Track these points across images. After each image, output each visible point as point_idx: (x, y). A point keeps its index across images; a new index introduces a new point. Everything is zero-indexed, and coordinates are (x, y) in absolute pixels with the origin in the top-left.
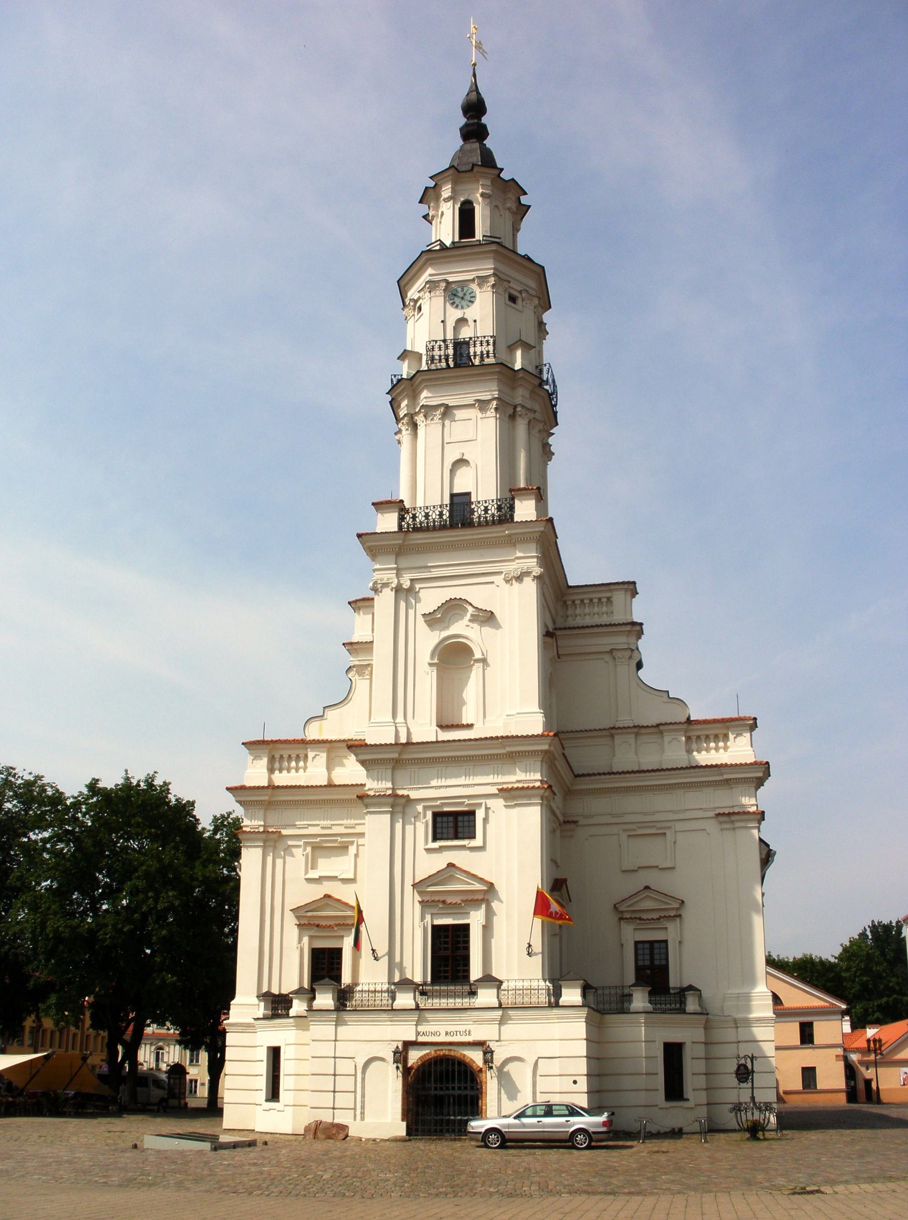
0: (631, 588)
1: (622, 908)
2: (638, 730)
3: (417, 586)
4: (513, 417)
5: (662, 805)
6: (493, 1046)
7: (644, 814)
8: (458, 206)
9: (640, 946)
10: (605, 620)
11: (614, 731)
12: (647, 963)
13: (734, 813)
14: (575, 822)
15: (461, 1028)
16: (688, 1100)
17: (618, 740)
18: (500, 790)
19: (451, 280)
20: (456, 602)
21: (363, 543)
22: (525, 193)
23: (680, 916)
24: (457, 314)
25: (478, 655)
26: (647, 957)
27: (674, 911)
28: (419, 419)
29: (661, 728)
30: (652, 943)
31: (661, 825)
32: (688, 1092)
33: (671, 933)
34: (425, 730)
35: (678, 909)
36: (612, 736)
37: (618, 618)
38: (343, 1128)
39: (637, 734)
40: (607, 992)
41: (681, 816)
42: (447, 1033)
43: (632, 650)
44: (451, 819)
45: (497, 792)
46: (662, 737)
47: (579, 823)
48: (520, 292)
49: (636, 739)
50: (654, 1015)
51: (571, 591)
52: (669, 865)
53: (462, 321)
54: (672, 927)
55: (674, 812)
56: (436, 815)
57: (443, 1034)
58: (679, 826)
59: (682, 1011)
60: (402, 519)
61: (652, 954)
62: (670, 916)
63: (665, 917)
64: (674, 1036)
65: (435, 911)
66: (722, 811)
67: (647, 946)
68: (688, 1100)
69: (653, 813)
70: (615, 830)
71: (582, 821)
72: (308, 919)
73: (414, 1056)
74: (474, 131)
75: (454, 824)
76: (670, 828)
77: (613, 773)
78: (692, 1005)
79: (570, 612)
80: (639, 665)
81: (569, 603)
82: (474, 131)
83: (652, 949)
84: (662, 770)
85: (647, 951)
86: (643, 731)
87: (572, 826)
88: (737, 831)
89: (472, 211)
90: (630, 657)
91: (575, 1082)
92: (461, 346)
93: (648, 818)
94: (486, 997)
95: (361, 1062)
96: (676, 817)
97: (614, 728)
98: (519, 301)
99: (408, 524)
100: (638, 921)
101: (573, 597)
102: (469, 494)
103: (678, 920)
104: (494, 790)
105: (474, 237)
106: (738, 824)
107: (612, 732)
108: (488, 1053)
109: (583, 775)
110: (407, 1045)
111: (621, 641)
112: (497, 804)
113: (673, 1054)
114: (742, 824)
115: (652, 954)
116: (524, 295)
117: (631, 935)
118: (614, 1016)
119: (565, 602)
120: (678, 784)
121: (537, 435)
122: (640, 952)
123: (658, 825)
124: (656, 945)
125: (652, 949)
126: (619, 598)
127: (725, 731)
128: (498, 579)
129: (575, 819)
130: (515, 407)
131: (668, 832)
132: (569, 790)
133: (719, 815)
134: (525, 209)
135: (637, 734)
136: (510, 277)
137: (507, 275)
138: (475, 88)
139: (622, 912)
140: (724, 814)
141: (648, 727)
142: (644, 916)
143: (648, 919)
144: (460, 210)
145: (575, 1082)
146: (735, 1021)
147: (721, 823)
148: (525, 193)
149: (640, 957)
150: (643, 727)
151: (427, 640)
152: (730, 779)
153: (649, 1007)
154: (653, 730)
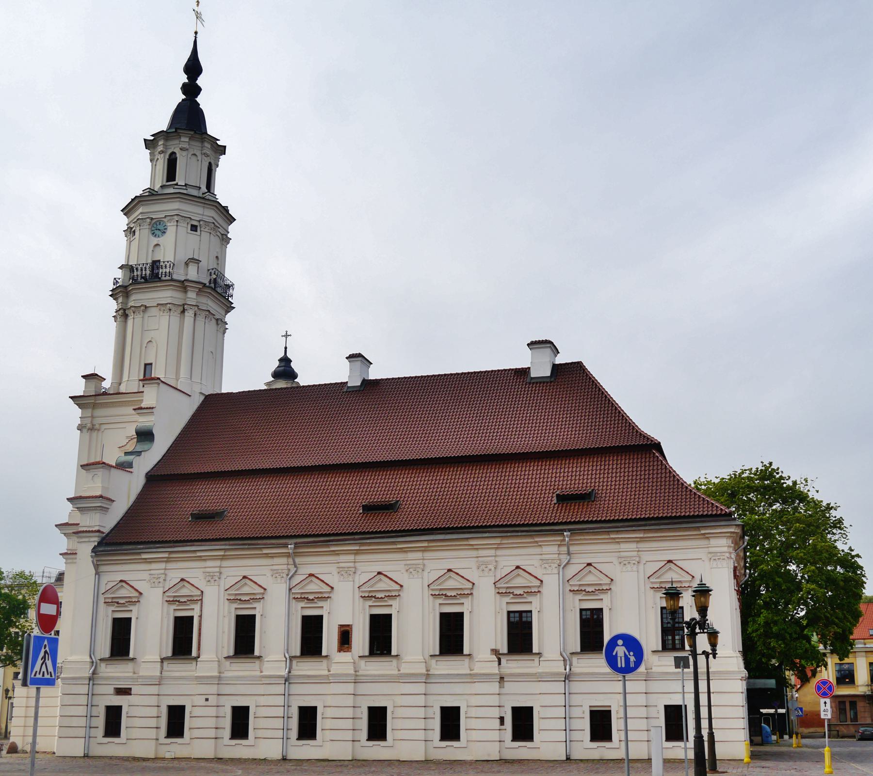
4: (183, 311)
8: (167, 157)
24: (155, 241)
28: (130, 313)
48: (199, 221)
53: (157, 245)
74: (191, 90)
82: (191, 90)
89: (176, 159)
92: (155, 264)
105: (174, 180)
144: (169, 160)
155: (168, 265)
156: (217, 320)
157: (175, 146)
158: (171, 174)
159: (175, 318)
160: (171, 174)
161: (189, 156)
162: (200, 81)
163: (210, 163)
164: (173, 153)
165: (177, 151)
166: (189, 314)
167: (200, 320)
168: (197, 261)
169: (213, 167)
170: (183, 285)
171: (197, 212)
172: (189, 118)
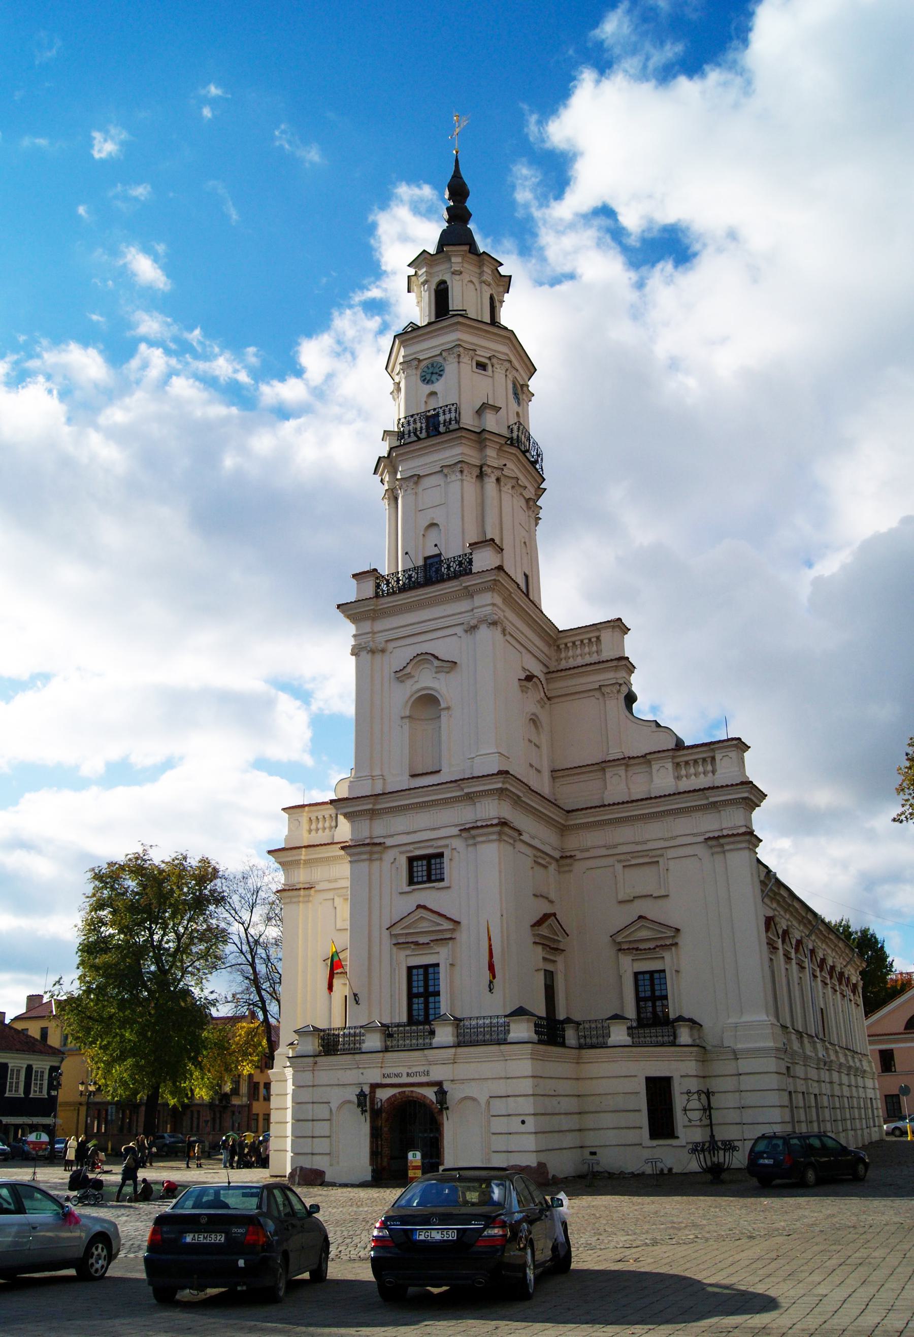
0: (618, 626)
1: (619, 939)
2: (627, 761)
3: (391, 646)
4: (481, 476)
5: (653, 833)
6: (446, 1086)
7: (637, 843)
8: (434, 287)
9: (640, 977)
10: (595, 658)
11: (604, 765)
12: (648, 994)
13: (724, 836)
14: (571, 856)
15: (421, 1069)
16: (678, 1137)
17: (609, 773)
18: (460, 830)
19: (421, 358)
21: (343, 612)
22: (501, 264)
23: (676, 944)
24: (428, 389)
25: (443, 705)
26: (648, 988)
27: (669, 938)
29: (648, 757)
30: (652, 973)
31: (654, 853)
32: (680, 1130)
33: (668, 962)
34: (399, 780)
35: (674, 937)
36: (603, 770)
37: (607, 654)
38: (321, 1174)
39: (627, 766)
40: (587, 1026)
41: (672, 843)
42: (408, 1075)
43: (620, 685)
44: (425, 862)
45: (458, 833)
46: (651, 767)
47: (577, 858)
48: (490, 358)
49: (626, 771)
50: (634, 1049)
51: (561, 635)
52: (663, 893)
53: (433, 394)
54: (667, 955)
55: (665, 839)
56: (411, 860)
57: (405, 1075)
58: (671, 853)
59: (673, 1044)
60: (378, 586)
61: (652, 984)
62: (666, 945)
63: (662, 946)
64: (658, 1069)
65: (408, 952)
66: (711, 835)
67: (647, 976)
68: (678, 1137)
69: (645, 842)
70: (610, 861)
71: (579, 855)
75: (426, 868)
76: (662, 855)
77: (605, 806)
78: (684, 1036)
79: (563, 655)
80: (631, 698)
81: (562, 646)
83: (652, 980)
84: (651, 798)
85: (647, 982)
86: (632, 762)
87: (568, 861)
88: (728, 855)
89: (446, 290)
90: (619, 691)
91: (523, 1122)
93: (639, 848)
94: (444, 1034)
95: (334, 1105)
96: (667, 844)
97: (605, 762)
98: (490, 367)
99: (383, 591)
100: (634, 952)
101: (565, 641)
102: (440, 555)
103: (673, 948)
104: (455, 831)
106: (727, 847)
107: (603, 766)
108: (442, 1093)
109: (573, 811)
110: (374, 1087)
111: (609, 677)
113: (659, 1090)
114: (731, 847)
115: (652, 984)
116: (494, 361)
117: (629, 966)
118: (588, 1051)
119: (558, 646)
120: (667, 811)
121: (510, 491)
122: (641, 983)
123: (651, 854)
124: (656, 975)
125: (652, 980)
126: (606, 636)
127: (710, 754)
128: (459, 630)
129: (573, 853)
130: (481, 467)
131: (661, 860)
132: (564, 826)
133: (709, 838)
134: (507, 279)
135: (627, 766)
136: (476, 345)
137: (472, 344)
138: (457, 175)
139: (619, 943)
140: (714, 838)
141: (638, 757)
142: (642, 946)
143: (645, 949)
145: (523, 1122)
146: (734, 1052)
147: (711, 847)
148: (501, 264)
149: (641, 989)
150: (633, 758)
151: (399, 697)
152: (717, 802)
153: (627, 1040)
154: (641, 760)
155: (453, 408)
156: (528, 501)
157: (442, 273)
159: (470, 485)
161: (465, 282)
162: (470, 204)
163: (492, 298)
164: (443, 282)
165: (447, 277)
166: (490, 484)
167: (507, 488)
168: (497, 409)
169: (497, 304)
170: (480, 437)
171: (487, 346)
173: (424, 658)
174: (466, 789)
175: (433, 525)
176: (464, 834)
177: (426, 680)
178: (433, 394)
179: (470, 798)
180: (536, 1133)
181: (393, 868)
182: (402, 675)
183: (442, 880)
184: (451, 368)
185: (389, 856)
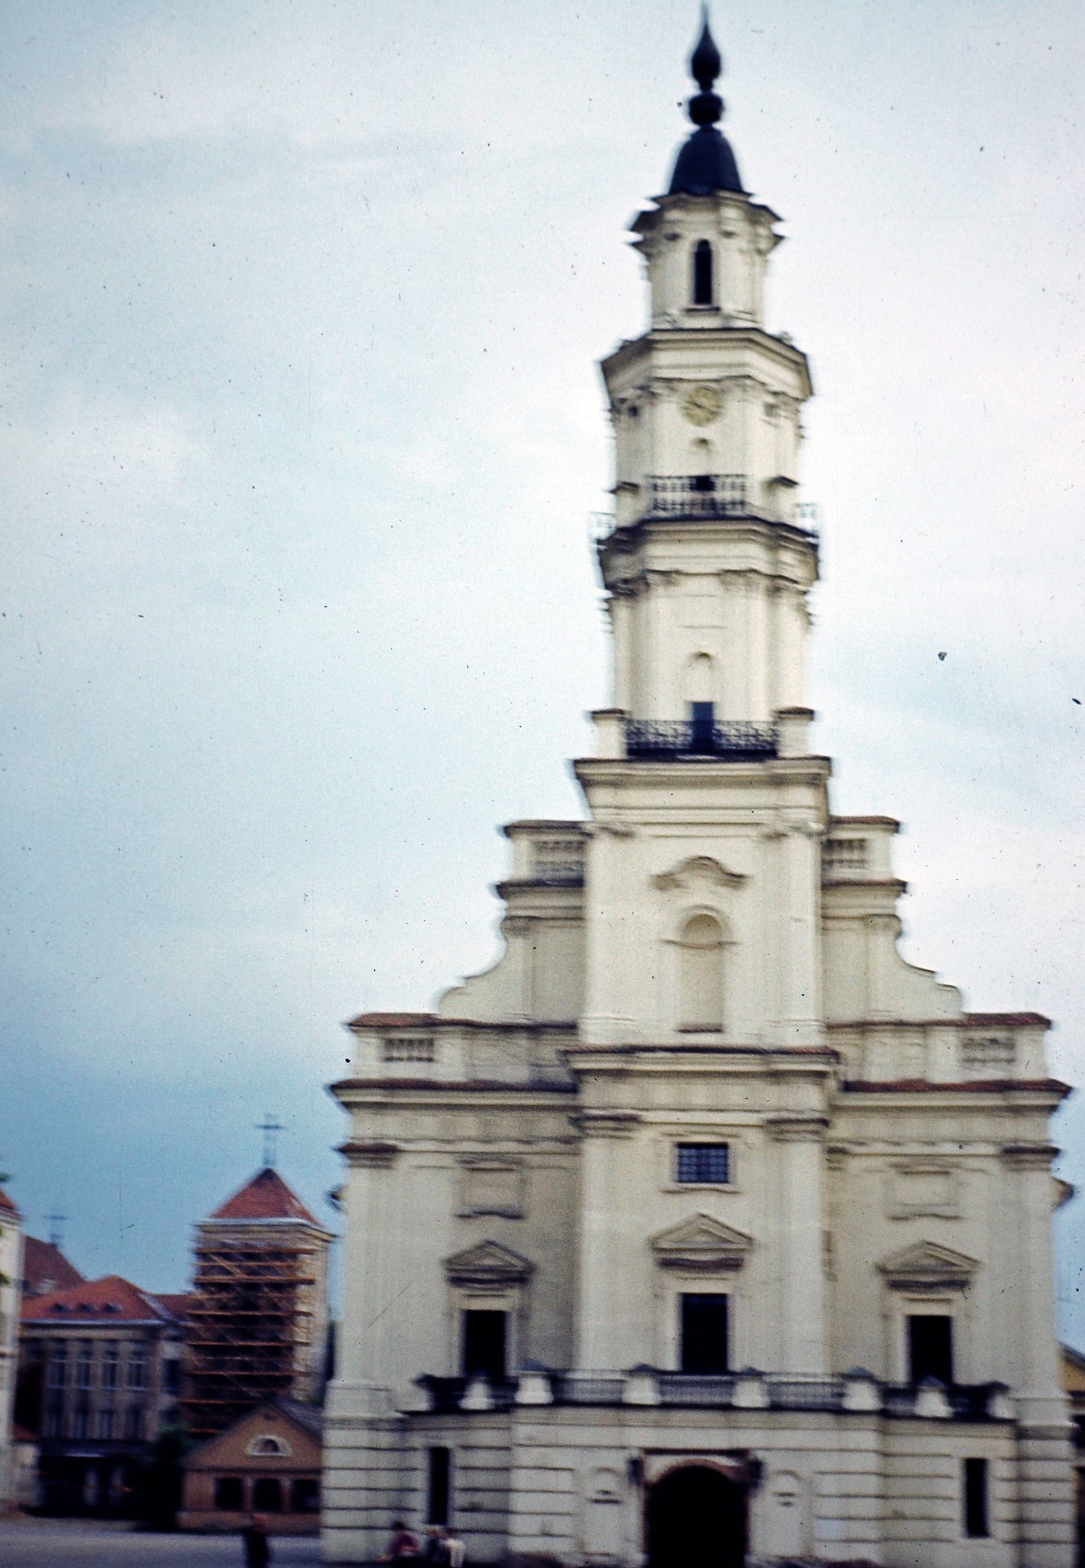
20: (705, 862)
72: (460, 1273)
73: (657, 1467)
74: (705, 109)
82: (705, 109)
92: (703, 483)
112: (755, 1137)
113: (975, 1472)
158: (703, 289)
160: (703, 289)
172: (705, 169)
173: (702, 864)
174: (770, 1063)
175: (704, 655)
176: (773, 1128)
177: (701, 893)
178: (704, 442)
179: (777, 1076)
180: (877, 1519)
181: (648, 1157)
182: (665, 882)
183: (726, 1181)
184: (733, 406)
185: (644, 1136)
